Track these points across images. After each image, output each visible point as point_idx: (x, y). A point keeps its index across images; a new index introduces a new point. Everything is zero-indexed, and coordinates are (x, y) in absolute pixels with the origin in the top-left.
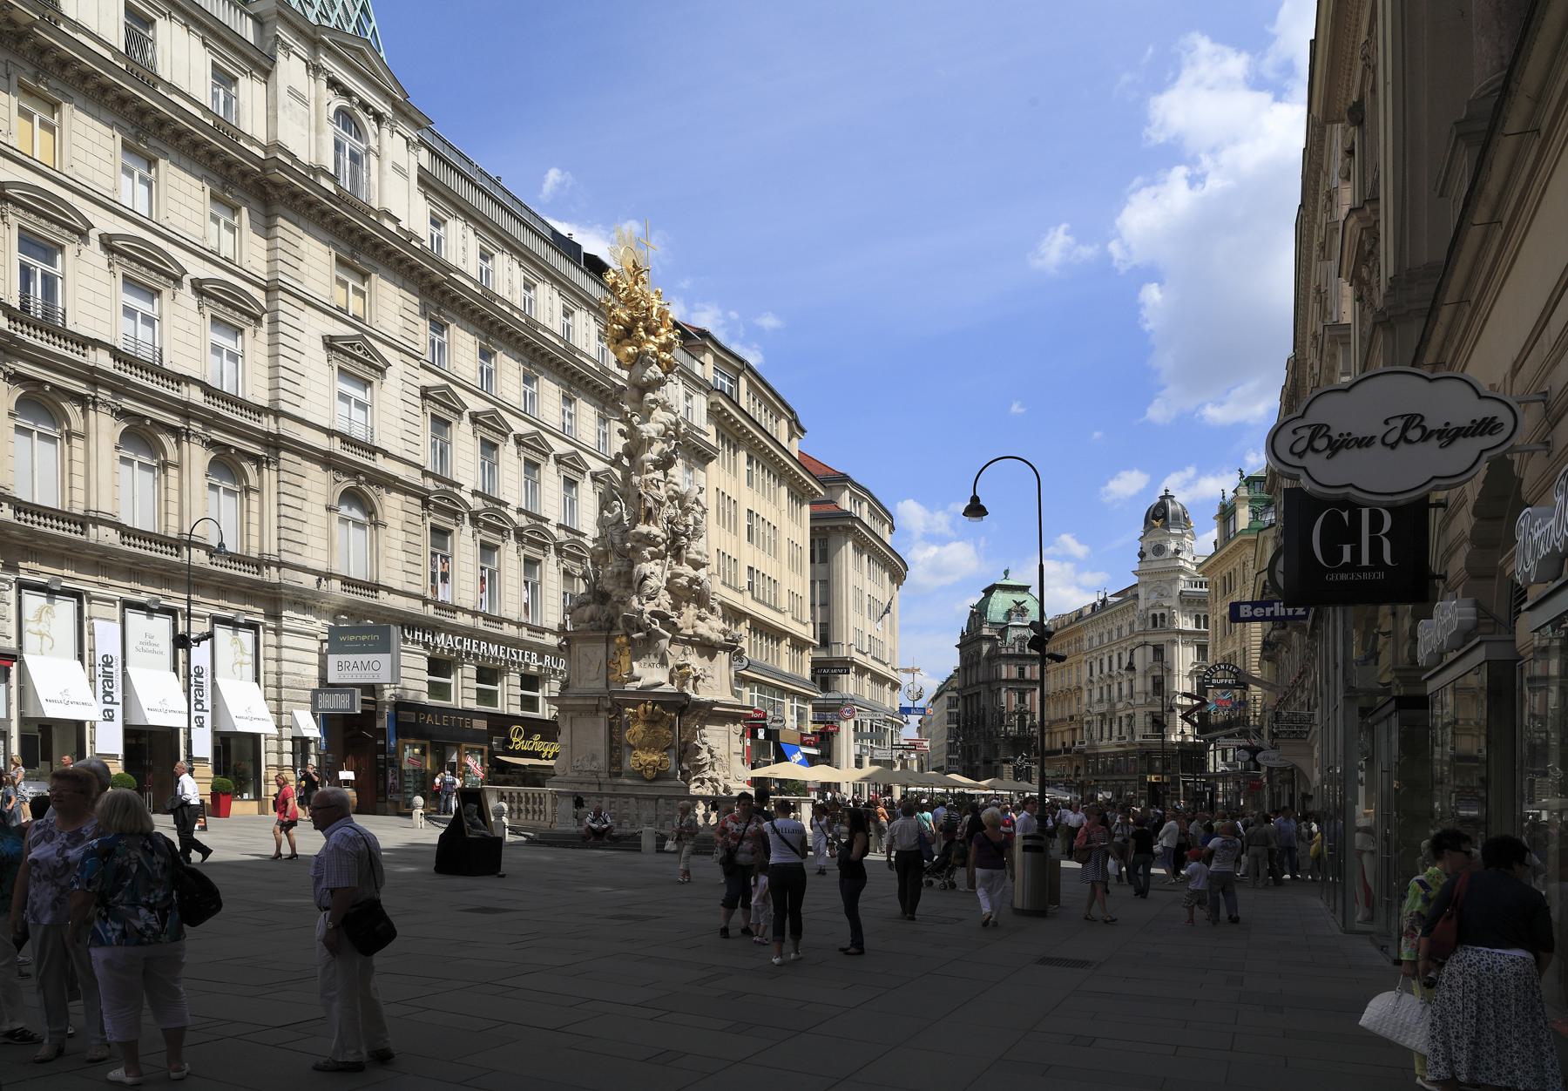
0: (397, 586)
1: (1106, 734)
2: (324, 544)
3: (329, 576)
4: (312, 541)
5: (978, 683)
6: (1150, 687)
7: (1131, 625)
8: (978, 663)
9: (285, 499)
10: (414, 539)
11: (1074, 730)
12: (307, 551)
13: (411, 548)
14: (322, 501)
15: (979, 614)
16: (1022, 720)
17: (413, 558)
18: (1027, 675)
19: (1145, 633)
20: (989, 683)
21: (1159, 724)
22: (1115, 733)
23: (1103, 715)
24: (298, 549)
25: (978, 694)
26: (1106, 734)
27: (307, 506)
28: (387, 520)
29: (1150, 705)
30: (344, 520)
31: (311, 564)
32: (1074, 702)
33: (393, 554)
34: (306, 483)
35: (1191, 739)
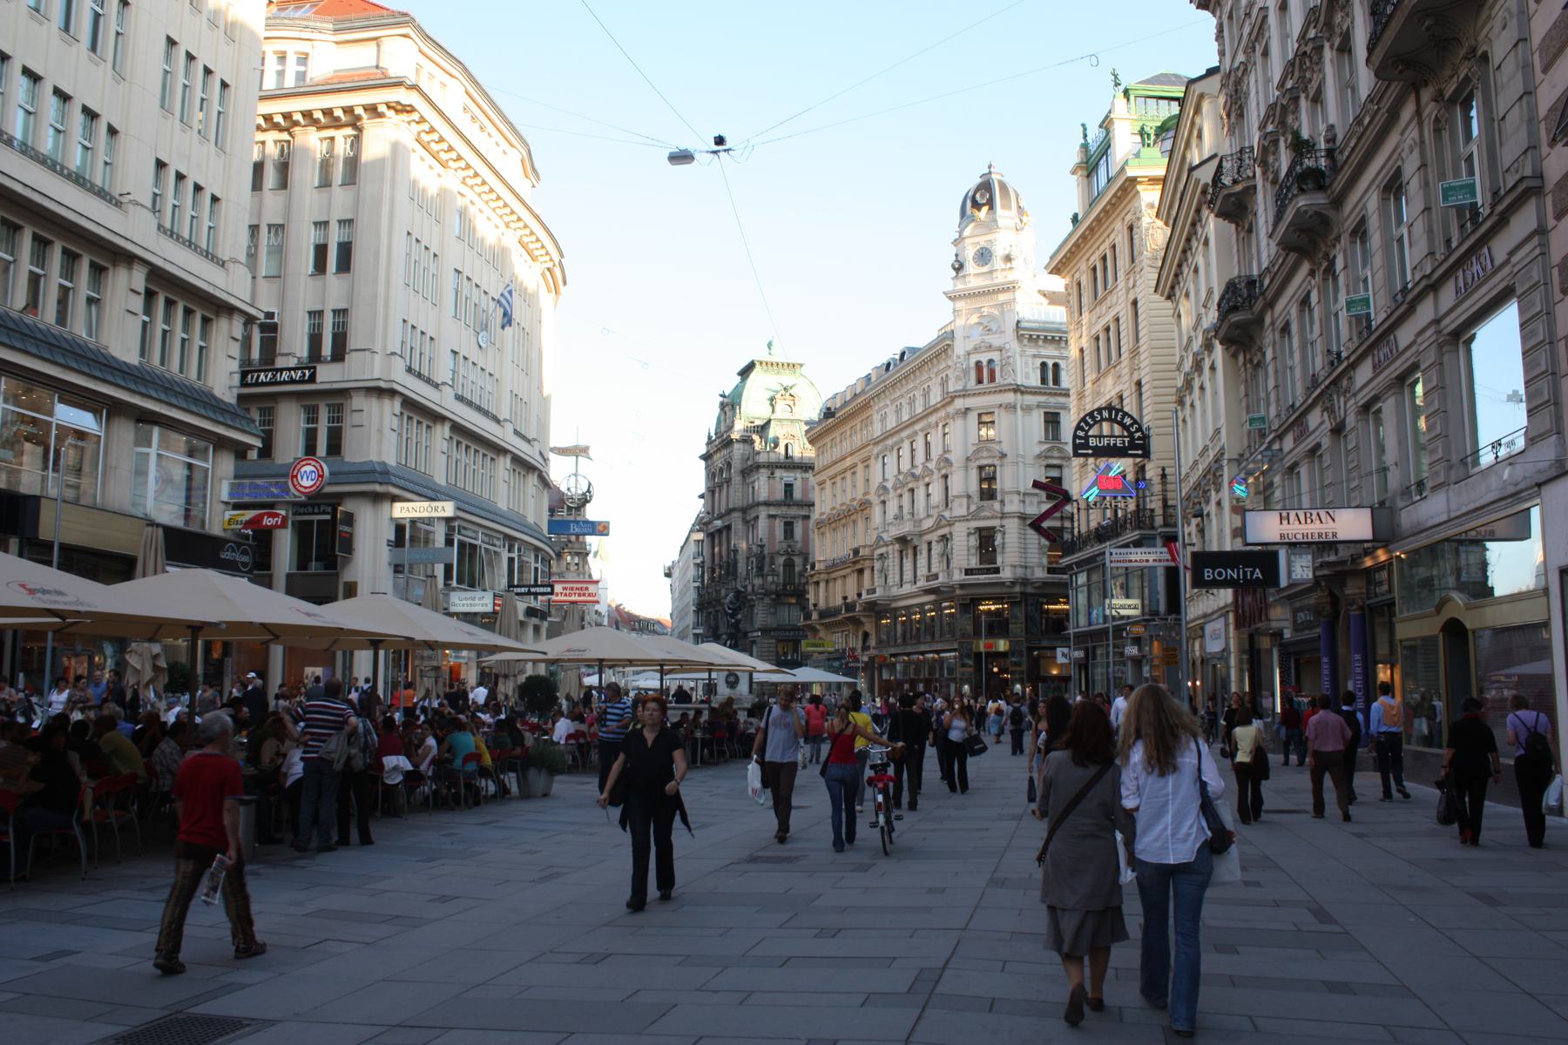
1: (908, 575)
5: (730, 511)
6: (974, 487)
7: (944, 382)
8: (728, 481)
11: (861, 571)
15: (730, 405)
16: (789, 565)
18: (797, 495)
19: (964, 394)
20: (744, 510)
21: (986, 541)
22: (922, 571)
23: (903, 540)
25: (728, 528)
26: (908, 575)
29: (974, 516)
32: (861, 524)
35: (1040, 574)
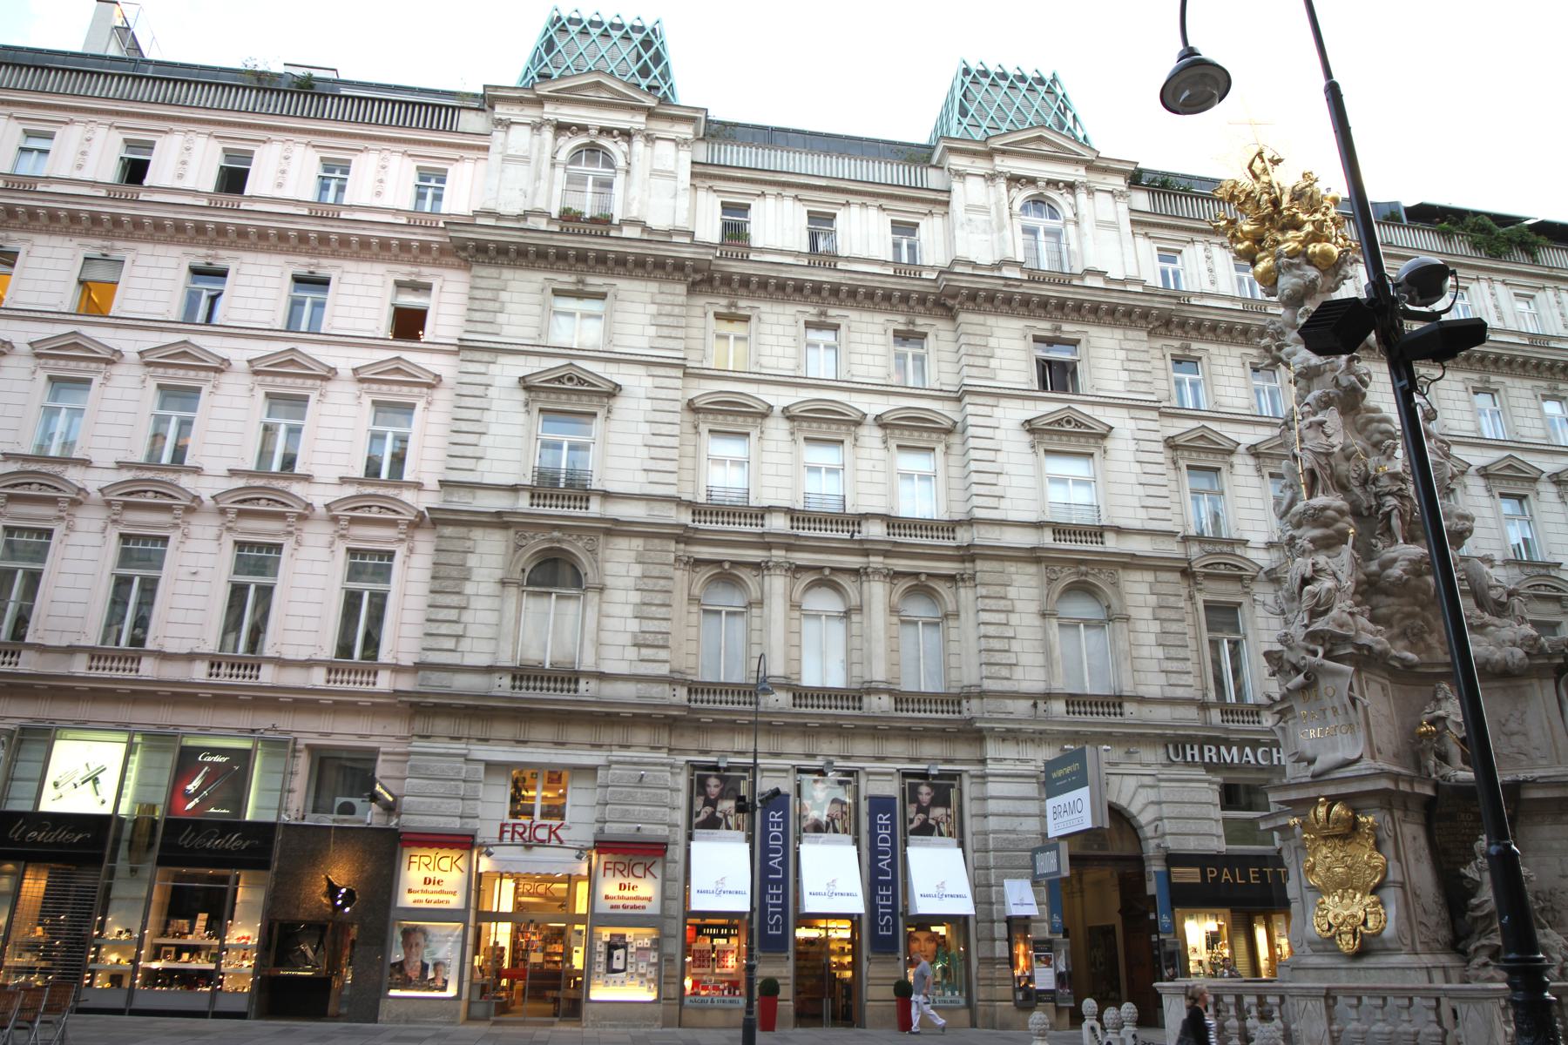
0: (1153, 691)
2: (1040, 659)
3: (1048, 696)
4: (1025, 659)
9: (985, 617)
10: (1174, 627)
12: (1018, 673)
13: (1171, 640)
14: (1034, 607)
17: (1173, 652)
24: (1004, 672)
27: (1014, 619)
28: (1133, 612)
30: (1069, 625)
31: (1025, 687)
33: (1145, 652)
34: (1012, 592)
